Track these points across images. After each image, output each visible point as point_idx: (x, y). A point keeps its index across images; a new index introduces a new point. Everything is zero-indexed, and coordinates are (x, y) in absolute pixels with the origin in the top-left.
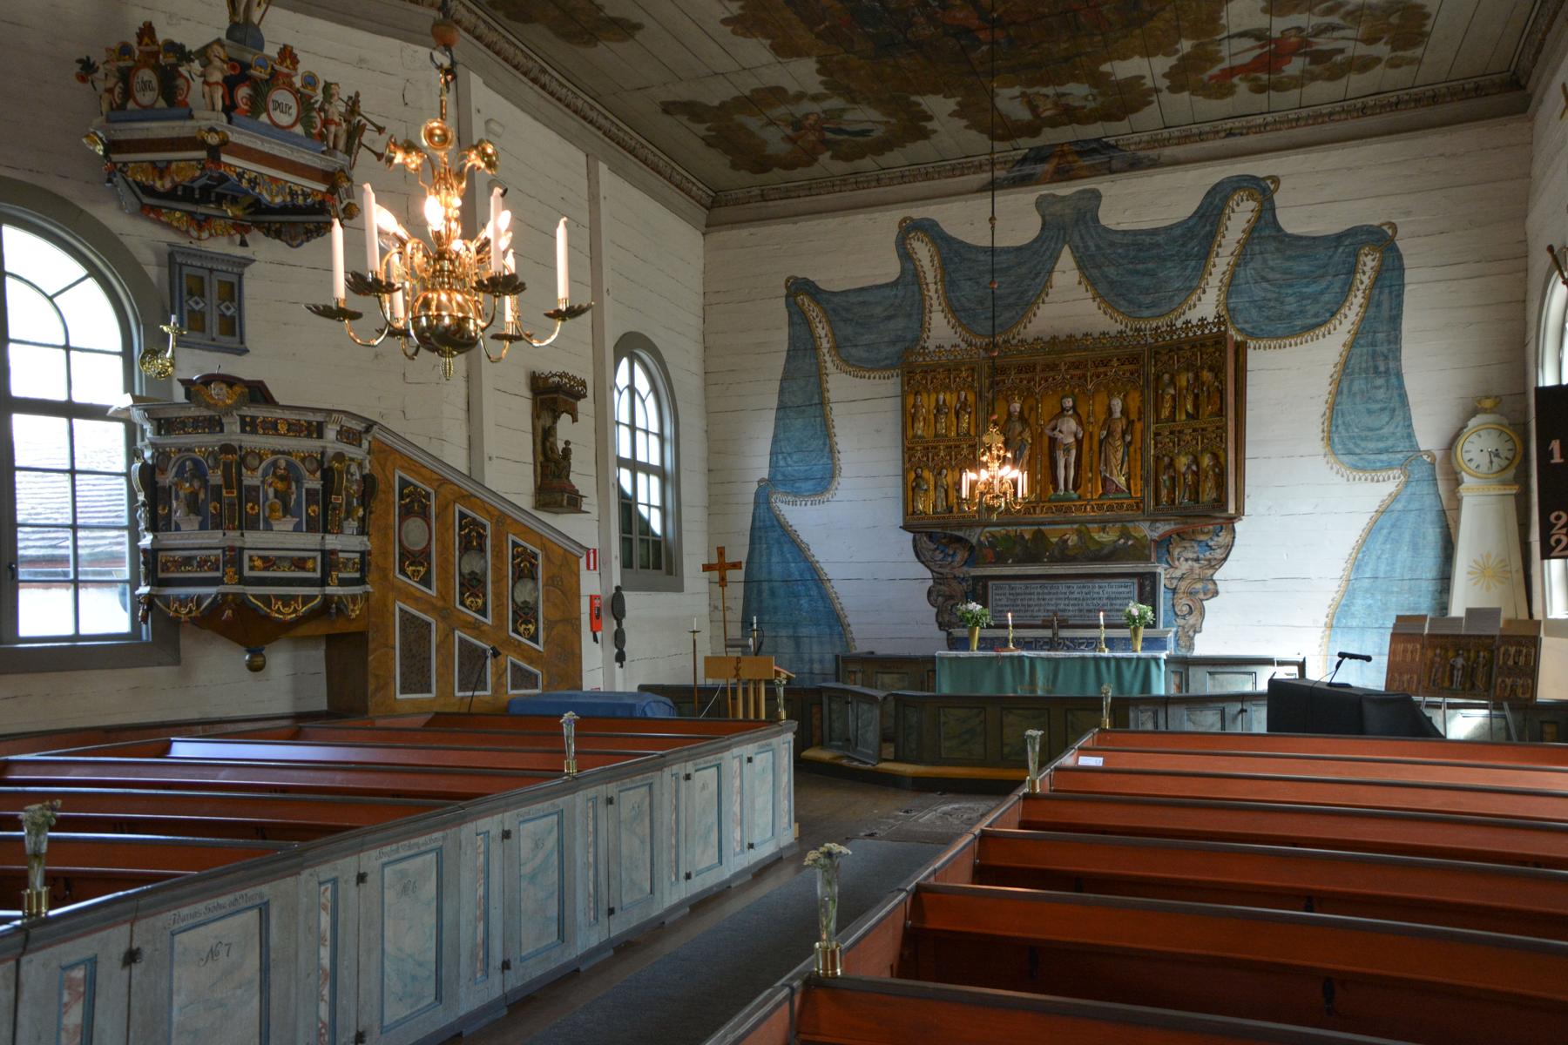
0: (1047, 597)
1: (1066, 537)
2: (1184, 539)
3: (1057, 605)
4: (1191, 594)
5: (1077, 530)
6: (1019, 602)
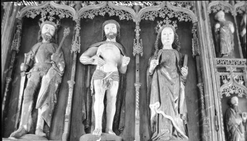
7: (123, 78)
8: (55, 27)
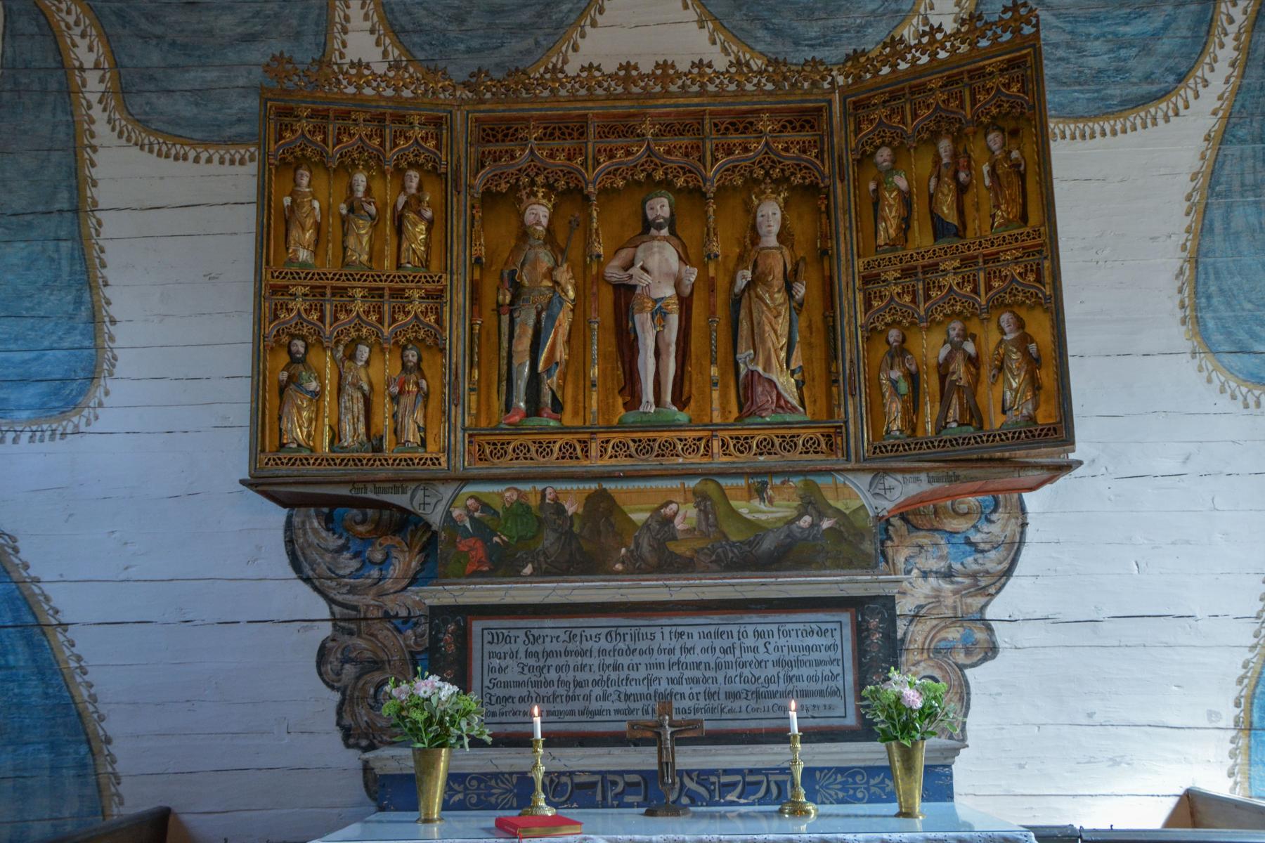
0: (624, 660)
2: (917, 529)
3: (650, 681)
4: (938, 652)
5: (695, 492)
6: (553, 675)
7: (685, 304)
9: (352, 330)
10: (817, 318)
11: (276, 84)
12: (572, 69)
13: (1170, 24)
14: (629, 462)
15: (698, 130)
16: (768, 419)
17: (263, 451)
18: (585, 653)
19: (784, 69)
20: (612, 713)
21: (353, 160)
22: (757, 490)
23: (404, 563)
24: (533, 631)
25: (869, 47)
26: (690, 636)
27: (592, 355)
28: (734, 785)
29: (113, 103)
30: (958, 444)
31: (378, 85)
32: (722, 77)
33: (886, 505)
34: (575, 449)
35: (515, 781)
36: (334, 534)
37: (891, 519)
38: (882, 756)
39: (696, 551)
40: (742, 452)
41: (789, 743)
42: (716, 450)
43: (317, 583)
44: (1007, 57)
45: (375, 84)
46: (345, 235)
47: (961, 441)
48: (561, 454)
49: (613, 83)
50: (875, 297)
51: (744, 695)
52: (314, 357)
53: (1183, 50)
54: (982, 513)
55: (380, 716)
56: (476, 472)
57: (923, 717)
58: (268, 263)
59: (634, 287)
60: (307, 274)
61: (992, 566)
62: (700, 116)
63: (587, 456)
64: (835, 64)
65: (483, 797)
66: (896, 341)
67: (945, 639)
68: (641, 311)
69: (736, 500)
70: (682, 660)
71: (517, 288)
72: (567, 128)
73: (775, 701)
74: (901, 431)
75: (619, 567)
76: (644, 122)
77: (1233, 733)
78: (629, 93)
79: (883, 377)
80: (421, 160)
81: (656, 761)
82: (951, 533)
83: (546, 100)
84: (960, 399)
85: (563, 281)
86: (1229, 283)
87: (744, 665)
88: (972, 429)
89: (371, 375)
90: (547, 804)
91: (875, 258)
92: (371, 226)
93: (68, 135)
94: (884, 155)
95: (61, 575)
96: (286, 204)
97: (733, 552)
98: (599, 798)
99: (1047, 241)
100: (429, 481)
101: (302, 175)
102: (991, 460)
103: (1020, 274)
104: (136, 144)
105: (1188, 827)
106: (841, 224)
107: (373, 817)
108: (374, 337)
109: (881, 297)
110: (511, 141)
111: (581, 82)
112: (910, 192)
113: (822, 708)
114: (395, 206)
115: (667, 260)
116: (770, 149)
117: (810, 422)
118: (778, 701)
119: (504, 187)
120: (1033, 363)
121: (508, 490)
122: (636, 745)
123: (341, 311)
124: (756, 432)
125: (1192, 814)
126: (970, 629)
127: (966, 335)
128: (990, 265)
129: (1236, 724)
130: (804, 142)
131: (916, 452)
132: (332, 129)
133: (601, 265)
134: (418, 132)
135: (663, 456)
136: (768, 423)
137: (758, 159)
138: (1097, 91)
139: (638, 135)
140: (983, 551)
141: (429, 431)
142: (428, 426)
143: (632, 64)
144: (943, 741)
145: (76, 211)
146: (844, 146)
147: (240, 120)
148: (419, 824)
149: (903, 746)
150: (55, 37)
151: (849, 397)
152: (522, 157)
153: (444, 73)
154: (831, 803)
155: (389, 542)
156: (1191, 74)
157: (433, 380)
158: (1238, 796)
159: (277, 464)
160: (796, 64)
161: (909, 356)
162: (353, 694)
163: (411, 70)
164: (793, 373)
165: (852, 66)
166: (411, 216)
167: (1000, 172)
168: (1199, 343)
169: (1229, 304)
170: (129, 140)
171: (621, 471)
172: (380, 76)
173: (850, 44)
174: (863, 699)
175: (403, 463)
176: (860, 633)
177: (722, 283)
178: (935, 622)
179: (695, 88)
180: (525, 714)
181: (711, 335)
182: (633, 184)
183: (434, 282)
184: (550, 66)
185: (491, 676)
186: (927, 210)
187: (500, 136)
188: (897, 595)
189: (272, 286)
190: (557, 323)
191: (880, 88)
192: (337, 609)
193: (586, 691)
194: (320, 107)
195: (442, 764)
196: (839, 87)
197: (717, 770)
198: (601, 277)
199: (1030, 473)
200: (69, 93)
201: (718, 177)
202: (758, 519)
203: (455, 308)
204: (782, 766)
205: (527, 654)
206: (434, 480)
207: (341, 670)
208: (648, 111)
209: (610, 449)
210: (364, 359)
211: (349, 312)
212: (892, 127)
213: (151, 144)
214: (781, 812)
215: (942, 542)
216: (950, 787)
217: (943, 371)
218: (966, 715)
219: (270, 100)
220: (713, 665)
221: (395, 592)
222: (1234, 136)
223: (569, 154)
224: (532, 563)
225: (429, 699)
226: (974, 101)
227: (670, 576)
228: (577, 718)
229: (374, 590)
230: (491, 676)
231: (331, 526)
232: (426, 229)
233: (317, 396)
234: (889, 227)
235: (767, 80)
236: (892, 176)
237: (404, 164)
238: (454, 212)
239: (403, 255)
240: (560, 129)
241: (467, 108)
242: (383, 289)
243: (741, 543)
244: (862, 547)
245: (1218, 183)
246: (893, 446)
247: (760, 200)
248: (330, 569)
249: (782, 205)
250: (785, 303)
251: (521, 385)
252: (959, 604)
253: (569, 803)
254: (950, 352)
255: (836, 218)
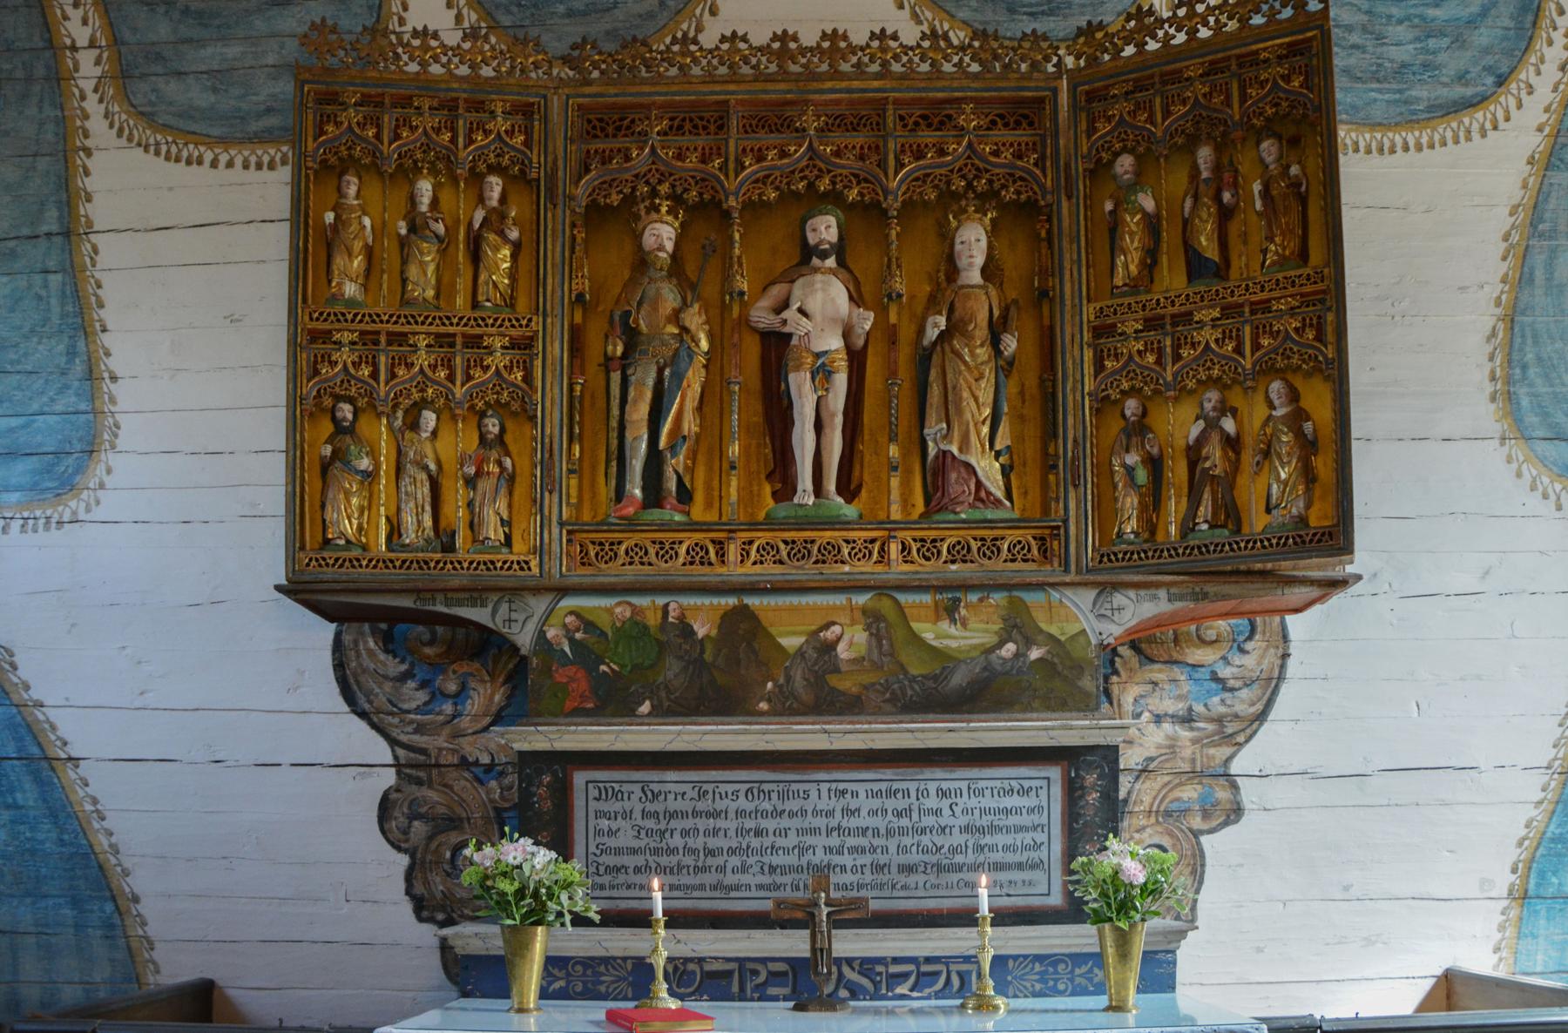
0: (770, 824)
1: (830, 634)
2: (1152, 661)
3: (802, 850)
4: (1169, 815)
5: (865, 611)
6: (677, 842)
7: (856, 359)
8: (675, 229)
9: (414, 390)
10: (1032, 381)
11: (315, 61)
12: (709, 39)
13: (1489, 9)
14: (778, 569)
15: (878, 124)
16: (963, 516)
17: (302, 548)
18: (719, 814)
19: (995, 45)
20: (753, 888)
21: (415, 162)
22: (946, 609)
23: (484, 696)
24: (652, 786)
25: (1107, 19)
26: (855, 794)
27: (731, 427)
28: (904, 976)
29: (111, 92)
30: (1208, 552)
31: (449, 61)
32: (911, 53)
33: (1113, 631)
34: (707, 552)
35: (629, 967)
36: (395, 657)
37: (1119, 649)
38: (1091, 941)
39: (866, 688)
40: (928, 559)
41: (977, 925)
42: (893, 555)
43: (375, 719)
44: (1287, 40)
45: (444, 59)
46: (404, 262)
47: (1212, 548)
48: (689, 559)
49: (764, 59)
50: (1109, 356)
51: (921, 869)
52: (365, 426)
53: (1504, 44)
54: (1234, 641)
55: (460, 885)
56: (576, 580)
57: (1145, 895)
58: (305, 300)
59: (789, 336)
60: (356, 315)
61: (1241, 708)
62: (880, 106)
63: (723, 562)
64: (1061, 40)
65: (590, 985)
66: (1133, 415)
67: (1178, 799)
68: (798, 368)
69: (918, 621)
70: (844, 824)
71: (632, 337)
72: (702, 119)
73: (961, 875)
74: (1137, 534)
75: (764, 706)
76: (805, 113)
77: (1505, 903)
78: (785, 72)
79: (1116, 462)
80: (506, 161)
81: (808, 946)
82: (1194, 666)
83: (673, 81)
84: (1214, 494)
85: (693, 327)
86: (1549, 349)
87: (923, 831)
88: (1226, 532)
89: (440, 451)
90: (670, 995)
91: (1109, 303)
92: (438, 251)
93: (57, 134)
94: (1125, 163)
95: (67, 699)
96: (327, 222)
97: (912, 689)
98: (735, 988)
99: (1332, 286)
100: (514, 592)
101: (348, 182)
102: (1249, 573)
103: (1296, 330)
104: (139, 145)
105: (1441, 1010)
106: (1067, 256)
107: (454, 1004)
108: (442, 400)
109: (1116, 355)
110: (626, 136)
111: (721, 57)
112: (1158, 216)
113: (1020, 884)
114: (470, 224)
115: (833, 300)
116: (974, 151)
117: (1018, 520)
118: (966, 876)
119: (615, 199)
120: (1308, 447)
121: (619, 604)
122: (783, 927)
123: (400, 364)
124: (947, 533)
125: (1448, 997)
126: (1211, 787)
127: (1225, 409)
128: (1259, 316)
129: (1510, 892)
130: (1019, 144)
131: (1155, 561)
132: (387, 120)
133: (745, 306)
134: (501, 124)
135: (824, 562)
136: (964, 521)
137: (957, 166)
138: (1400, 91)
139: (797, 130)
140: (1232, 690)
141: (514, 524)
142: (514, 518)
143: (791, 33)
144: (1169, 922)
145: (67, 234)
146: (1072, 152)
147: (269, 110)
148: (512, 1014)
149: (1118, 929)
150: (43, 9)
151: (1071, 489)
152: (640, 158)
153: (537, 45)
154: (1026, 996)
155: (465, 669)
156: (1513, 76)
157: (519, 459)
158: (1501, 973)
159: (320, 566)
160: (1010, 39)
161: (1151, 436)
162: (424, 858)
163: (493, 40)
164: (998, 455)
165: (1085, 43)
166: (492, 237)
167: (1274, 193)
168: (1509, 425)
169: (1547, 377)
170: (130, 139)
171: (768, 582)
172: (452, 49)
173: (1083, 14)
174: (1072, 873)
175: (482, 567)
176: (1073, 791)
177: (906, 333)
178: (1167, 778)
179: (875, 68)
180: (642, 887)
181: (890, 402)
182: (789, 197)
183: (521, 326)
184: (679, 35)
185: (598, 840)
186: (1179, 241)
187: (610, 130)
188: (1121, 745)
189: (310, 332)
190: (685, 384)
191: (1119, 74)
192: (401, 752)
193: (720, 861)
194: (373, 91)
195: (538, 946)
196: (1068, 71)
197: (885, 958)
198: (744, 322)
199: (1296, 590)
200: (58, 80)
201: (904, 188)
202: (947, 647)
203: (549, 362)
204: (966, 954)
205: (645, 814)
206: (523, 589)
207: (409, 827)
208: (811, 97)
209: (753, 553)
210: (430, 429)
211: (409, 366)
212: (1137, 128)
213: (157, 144)
214: (963, 1006)
215: (1183, 678)
216: (1173, 976)
217: (1194, 454)
218: (1197, 891)
219: (308, 82)
220: (883, 831)
221: (474, 733)
222: (1561, 160)
223: (703, 154)
224: (651, 699)
225: (519, 867)
226: (1244, 97)
227: (830, 718)
228: (708, 894)
229: (447, 730)
230: (598, 840)
231: (390, 647)
232: (512, 256)
233: (370, 477)
234: (1129, 263)
235: (971, 59)
236: (1135, 193)
237: (482, 167)
238: (549, 232)
239: (480, 290)
240: (691, 120)
241: (567, 91)
242: (454, 335)
243: (922, 676)
244: (1080, 684)
245: (1541, 220)
246: (1125, 553)
247: (959, 221)
248: (390, 702)
249: (989, 228)
250: (989, 361)
251: (637, 465)
252: (1198, 756)
253: (698, 994)
254: (1203, 432)
255: (1060, 249)
